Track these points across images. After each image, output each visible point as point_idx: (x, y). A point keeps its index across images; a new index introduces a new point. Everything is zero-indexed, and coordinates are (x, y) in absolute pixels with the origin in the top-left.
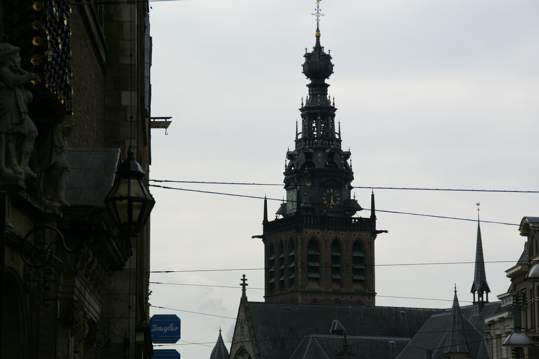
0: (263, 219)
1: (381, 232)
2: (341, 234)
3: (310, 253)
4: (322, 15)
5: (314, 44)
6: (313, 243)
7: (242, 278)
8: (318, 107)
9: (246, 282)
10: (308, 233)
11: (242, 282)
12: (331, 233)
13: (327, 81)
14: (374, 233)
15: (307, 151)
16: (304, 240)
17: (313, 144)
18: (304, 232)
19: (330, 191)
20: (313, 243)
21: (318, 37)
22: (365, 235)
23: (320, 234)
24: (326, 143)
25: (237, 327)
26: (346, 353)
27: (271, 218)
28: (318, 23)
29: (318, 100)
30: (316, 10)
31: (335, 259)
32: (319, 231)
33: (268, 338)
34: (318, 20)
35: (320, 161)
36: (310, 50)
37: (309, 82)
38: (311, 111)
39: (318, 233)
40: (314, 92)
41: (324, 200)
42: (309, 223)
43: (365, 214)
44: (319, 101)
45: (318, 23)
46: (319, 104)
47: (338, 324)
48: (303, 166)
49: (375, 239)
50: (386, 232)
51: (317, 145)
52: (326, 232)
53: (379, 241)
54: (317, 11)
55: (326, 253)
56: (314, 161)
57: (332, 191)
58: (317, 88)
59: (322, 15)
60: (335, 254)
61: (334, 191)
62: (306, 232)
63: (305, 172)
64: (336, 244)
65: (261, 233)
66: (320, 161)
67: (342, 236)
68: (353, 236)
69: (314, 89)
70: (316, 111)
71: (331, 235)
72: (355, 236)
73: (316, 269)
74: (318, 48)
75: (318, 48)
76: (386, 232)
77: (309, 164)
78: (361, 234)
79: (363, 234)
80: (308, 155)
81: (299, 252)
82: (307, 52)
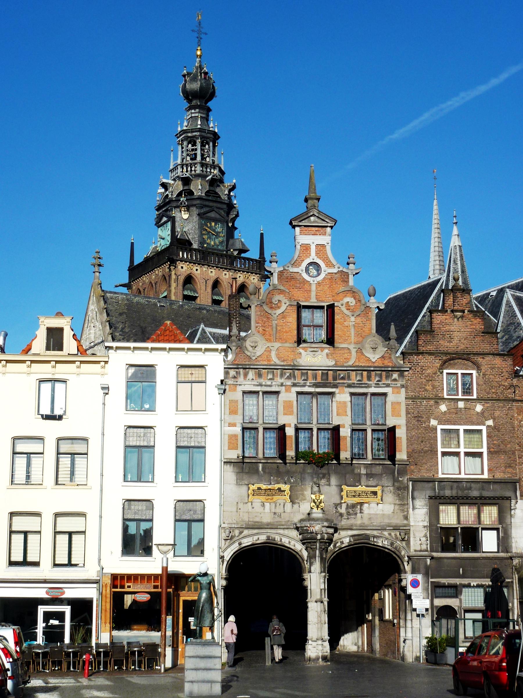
0: (128, 265)
2: (224, 274)
3: (186, 293)
4: (204, 33)
8: (199, 128)
10: (185, 268)
16: (179, 277)
18: (179, 267)
19: (211, 224)
22: (253, 280)
23: (199, 270)
24: (206, 172)
25: (85, 329)
26: (313, 215)
27: (138, 260)
29: (198, 121)
30: (197, 26)
32: (197, 268)
34: (199, 39)
38: (190, 135)
39: (197, 270)
40: (193, 115)
41: (205, 234)
43: (254, 254)
44: (199, 123)
46: (199, 126)
48: (180, 194)
51: (197, 172)
56: (192, 188)
57: (213, 224)
58: (197, 110)
59: (204, 33)
60: (215, 297)
61: (215, 225)
62: (182, 267)
63: (182, 199)
65: (126, 281)
67: (226, 276)
69: (193, 111)
70: (194, 134)
71: (213, 273)
72: (241, 278)
78: (248, 278)
80: (186, 181)
81: (173, 290)
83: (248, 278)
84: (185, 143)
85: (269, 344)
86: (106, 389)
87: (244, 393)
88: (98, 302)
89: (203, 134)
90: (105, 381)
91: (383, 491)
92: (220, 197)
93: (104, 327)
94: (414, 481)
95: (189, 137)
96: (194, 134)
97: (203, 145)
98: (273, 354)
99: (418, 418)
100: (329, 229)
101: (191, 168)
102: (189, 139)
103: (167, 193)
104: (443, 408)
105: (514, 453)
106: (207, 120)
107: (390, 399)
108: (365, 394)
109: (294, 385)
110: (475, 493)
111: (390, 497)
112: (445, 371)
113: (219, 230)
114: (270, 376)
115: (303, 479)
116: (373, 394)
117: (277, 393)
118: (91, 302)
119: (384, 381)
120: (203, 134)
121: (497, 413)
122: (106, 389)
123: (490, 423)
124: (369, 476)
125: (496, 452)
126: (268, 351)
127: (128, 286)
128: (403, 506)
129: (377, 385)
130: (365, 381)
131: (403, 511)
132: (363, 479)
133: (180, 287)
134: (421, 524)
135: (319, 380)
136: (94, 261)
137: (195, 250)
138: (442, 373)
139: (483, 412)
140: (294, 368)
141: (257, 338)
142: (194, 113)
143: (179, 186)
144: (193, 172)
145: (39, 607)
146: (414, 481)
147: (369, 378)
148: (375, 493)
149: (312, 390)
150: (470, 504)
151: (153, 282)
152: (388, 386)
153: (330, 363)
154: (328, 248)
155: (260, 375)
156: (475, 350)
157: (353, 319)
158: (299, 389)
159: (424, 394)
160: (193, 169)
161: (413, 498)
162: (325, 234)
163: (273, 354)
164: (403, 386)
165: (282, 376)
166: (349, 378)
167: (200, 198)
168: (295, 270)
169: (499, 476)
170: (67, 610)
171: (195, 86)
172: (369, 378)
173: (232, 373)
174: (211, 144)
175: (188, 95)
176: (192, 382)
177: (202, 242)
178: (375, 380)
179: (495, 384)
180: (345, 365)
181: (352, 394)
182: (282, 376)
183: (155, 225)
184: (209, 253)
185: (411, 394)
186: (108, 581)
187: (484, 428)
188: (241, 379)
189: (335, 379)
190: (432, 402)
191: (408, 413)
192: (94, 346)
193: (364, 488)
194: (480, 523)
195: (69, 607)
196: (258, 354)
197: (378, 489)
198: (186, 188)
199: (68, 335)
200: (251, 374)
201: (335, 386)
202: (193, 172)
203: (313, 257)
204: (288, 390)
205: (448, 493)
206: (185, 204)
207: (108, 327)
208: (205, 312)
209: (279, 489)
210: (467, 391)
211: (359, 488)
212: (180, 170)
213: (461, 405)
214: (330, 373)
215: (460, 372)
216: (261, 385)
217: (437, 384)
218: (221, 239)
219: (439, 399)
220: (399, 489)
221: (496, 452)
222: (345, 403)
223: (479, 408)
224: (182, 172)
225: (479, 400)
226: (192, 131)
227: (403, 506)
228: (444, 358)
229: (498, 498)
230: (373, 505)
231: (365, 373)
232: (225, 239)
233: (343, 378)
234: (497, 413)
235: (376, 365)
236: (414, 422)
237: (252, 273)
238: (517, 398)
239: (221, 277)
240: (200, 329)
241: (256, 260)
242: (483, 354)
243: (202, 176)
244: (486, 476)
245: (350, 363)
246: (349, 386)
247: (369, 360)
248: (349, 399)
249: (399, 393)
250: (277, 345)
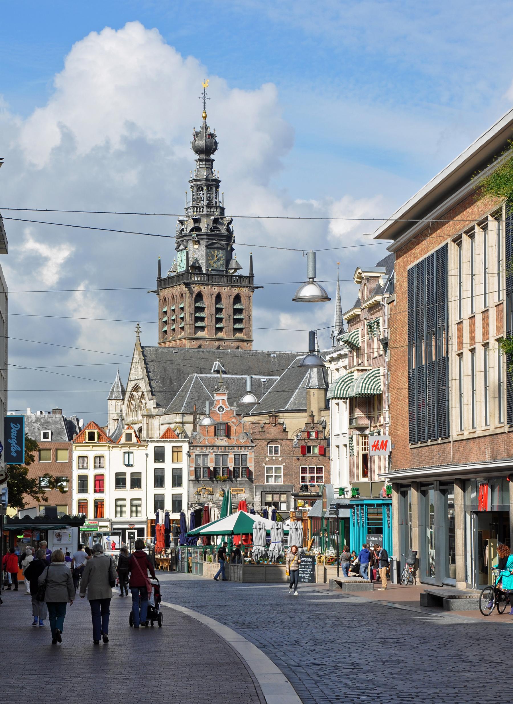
4: (208, 98)
5: (202, 124)
7: (137, 326)
9: (140, 329)
11: (136, 329)
13: (212, 157)
14: (253, 289)
15: (195, 217)
17: (200, 211)
22: (244, 292)
24: (211, 211)
25: (132, 368)
27: (164, 276)
28: (204, 105)
30: (202, 94)
31: (219, 311)
33: (158, 377)
34: (205, 103)
37: (197, 157)
38: (198, 183)
39: (204, 288)
40: (201, 166)
43: (245, 272)
45: (204, 105)
47: (219, 366)
48: (192, 230)
50: (263, 287)
51: (204, 212)
54: (203, 95)
56: (201, 226)
63: (193, 235)
67: (225, 291)
68: (234, 291)
69: (201, 163)
70: (202, 182)
71: (216, 290)
72: (236, 291)
78: (241, 290)
79: (242, 289)
80: (196, 221)
83: (241, 290)
84: (195, 189)
85: (205, 437)
86: (147, 455)
87: (196, 455)
88: (139, 355)
89: (209, 183)
90: (147, 452)
91: (245, 489)
92: (220, 231)
93: (143, 371)
94: (256, 486)
95: (198, 185)
96: (202, 182)
98: (206, 441)
99: (258, 463)
100: (227, 394)
101: (200, 209)
103: (183, 227)
104: (267, 459)
105: (292, 475)
106: (212, 168)
107: (248, 456)
108: (239, 455)
109: (214, 452)
110: (278, 490)
111: (247, 491)
112: (269, 446)
113: (220, 255)
114: (205, 449)
115: (217, 486)
116: (242, 455)
117: (208, 455)
118: (135, 353)
119: (246, 450)
120: (209, 183)
121: (287, 461)
122: (147, 455)
123: (284, 464)
124: (240, 484)
125: (286, 475)
126: (205, 440)
127: (157, 292)
128: (252, 494)
129: (244, 452)
130: (239, 450)
131: (252, 496)
132: (238, 485)
133: (193, 302)
134: (258, 501)
135: (223, 450)
136: (136, 329)
137: (204, 274)
138: (267, 446)
139: (282, 460)
140: (214, 446)
141: (201, 435)
142: (201, 165)
143: (191, 225)
144: (201, 213)
145: (127, 531)
146: (256, 486)
147: (241, 449)
148: (242, 490)
149: (220, 454)
150: (276, 494)
151: (174, 295)
152: (248, 452)
153: (227, 444)
154: (226, 400)
155: (202, 449)
156: (280, 438)
157: (235, 427)
158: (216, 454)
159: (260, 454)
160: (201, 210)
161: (256, 492)
162: (225, 396)
163: (206, 441)
164: (253, 452)
165: (209, 449)
166: (234, 449)
167: (207, 234)
168: (214, 409)
169: (287, 483)
170: (136, 531)
171: (201, 143)
172: (241, 449)
173: (192, 448)
174: (214, 189)
175: (198, 151)
176: (177, 452)
177: (208, 266)
178: (243, 449)
179: (286, 450)
180: (232, 444)
181: (235, 455)
182: (209, 449)
183: (175, 249)
184: (213, 275)
185: (256, 455)
186: (150, 522)
187: (282, 466)
188: (195, 450)
189: (228, 449)
190: (263, 457)
191: (254, 461)
192: (138, 380)
193: (238, 489)
194: (280, 500)
195: (136, 531)
196: (201, 441)
197: (243, 489)
198: (196, 225)
199: (133, 435)
200: (198, 448)
201: (229, 452)
203: (221, 405)
204: (212, 454)
205: (268, 490)
206: (195, 238)
207: (145, 371)
208: (201, 353)
209: (208, 489)
210: (276, 452)
211: (237, 489)
212: (191, 210)
213: (274, 458)
214: (227, 448)
215: (274, 446)
216: (202, 452)
217: (265, 450)
218: (222, 262)
219: (266, 456)
220: (251, 488)
221: (286, 475)
222: (232, 458)
223: (280, 459)
224: (194, 212)
225: (280, 456)
226: (200, 180)
227: (252, 494)
228: (269, 441)
229: (287, 491)
230: (242, 494)
231: (239, 448)
232: (225, 262)
233: (232, 449)
234: (287, 461)
235: (243, 444)
236: (257, 464)
237: (244, 287)
238: (295, 455)
239: (221, 292)
240: (195, 377)
241: (247, 277)
242: (282, 440)
243: (208, 215)
244: (282, 484)
245: (234, 444)
246: (234, 452)
247: (241, 442)
248: (233, 457)
249: (251, 454)
250: (208, 437)
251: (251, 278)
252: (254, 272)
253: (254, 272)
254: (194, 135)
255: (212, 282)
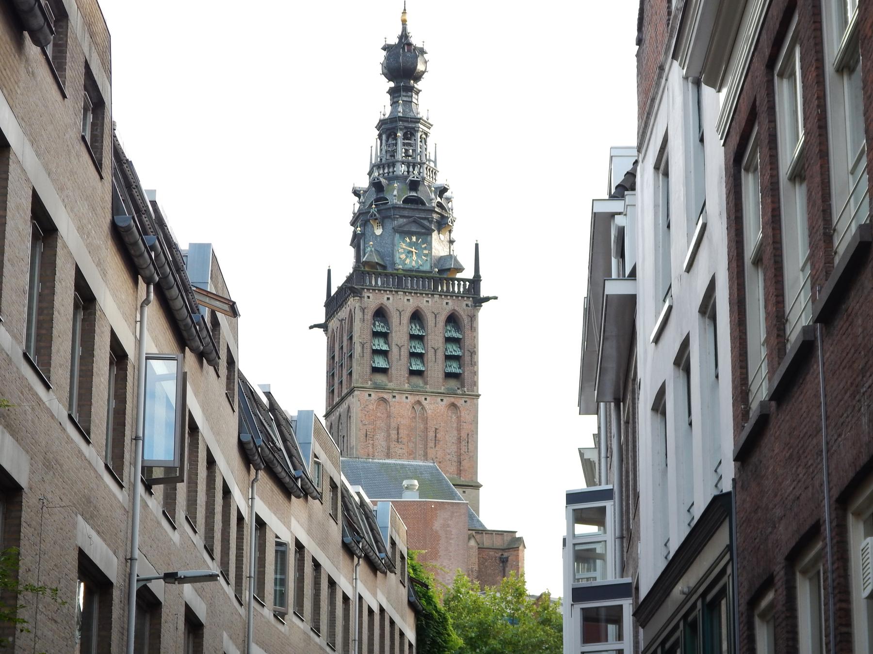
1: (487, 299)
6: (381, 314)
12: (408, 300)
14: (479, 301)
19: (411, 239)
20: (381, 314)
21: (404, 22)
32: (388, 296)
35: (396, 195)
36: (394, 40)
39: (388, 299)
42: (373, 283)
43: (468, 273)
49: (478, 310)
50: (496, 298)
52: (402, 297)
53: (485, 313)
55: (400, 330)
57: (414, 239)
61: (417, 239)
64: (417, 317)
66: (396, 195)
67: (427, 304)
73: (384, 353)
74: (404, 36)
75: (404, 36)
76: (496, 298)
77: (381, 200)
82: (387, 43)
97: (405, 137)
102: (388, 132)
167: (395, 207)
202: (391, 174)
239: (420, 305)
251: (476, 281)
252: (481, 273)
253: (481, 273)
254: (384, 49)
255: (404, 289)
